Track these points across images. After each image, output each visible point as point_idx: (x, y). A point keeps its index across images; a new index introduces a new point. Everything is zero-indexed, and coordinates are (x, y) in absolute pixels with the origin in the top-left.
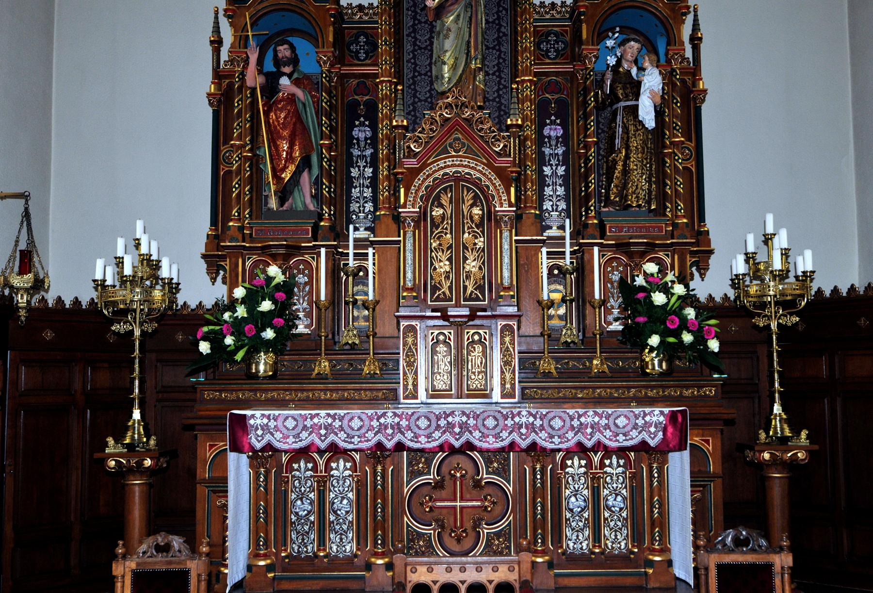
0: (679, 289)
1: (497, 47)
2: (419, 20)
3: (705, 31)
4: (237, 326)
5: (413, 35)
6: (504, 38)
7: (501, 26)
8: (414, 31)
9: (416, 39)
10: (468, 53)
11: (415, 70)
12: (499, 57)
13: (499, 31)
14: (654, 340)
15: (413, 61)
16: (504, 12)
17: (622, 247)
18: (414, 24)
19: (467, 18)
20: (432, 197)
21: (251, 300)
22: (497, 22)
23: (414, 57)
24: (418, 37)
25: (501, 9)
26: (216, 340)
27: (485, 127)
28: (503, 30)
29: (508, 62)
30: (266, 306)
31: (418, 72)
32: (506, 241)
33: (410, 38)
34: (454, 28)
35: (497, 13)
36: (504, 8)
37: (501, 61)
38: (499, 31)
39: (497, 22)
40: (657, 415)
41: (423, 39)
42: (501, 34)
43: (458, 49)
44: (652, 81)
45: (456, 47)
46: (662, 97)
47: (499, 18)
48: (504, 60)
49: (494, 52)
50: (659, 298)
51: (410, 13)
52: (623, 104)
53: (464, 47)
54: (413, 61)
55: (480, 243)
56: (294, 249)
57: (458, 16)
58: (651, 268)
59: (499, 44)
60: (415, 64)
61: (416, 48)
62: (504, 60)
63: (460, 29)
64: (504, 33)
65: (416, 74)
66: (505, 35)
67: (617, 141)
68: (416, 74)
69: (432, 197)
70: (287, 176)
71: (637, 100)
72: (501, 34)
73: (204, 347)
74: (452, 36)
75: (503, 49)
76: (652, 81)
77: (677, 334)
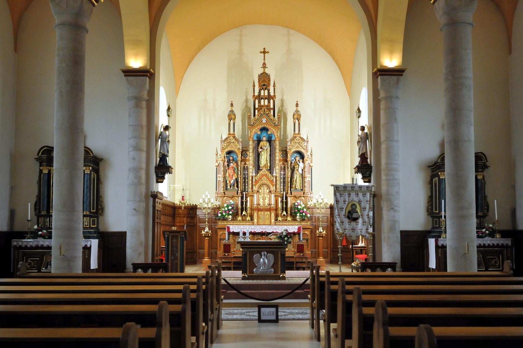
0: (303, 206)
3: (313, 153)
4: (225, 211)
14: (298, 214)
17: (295, 197)
20: (260, 187)
21: (227, 206)
26: (221, 213)
30: (230, 208)
32: (273, 196)
40: (297, 227)
44: (301, 165)
50: (299, 207)
55: (268, 196)
56: (233, 196)
58: (299, 201)
69: (260, 187)
70: (232, 182)
73: (220, 215)
77: (302, 213)
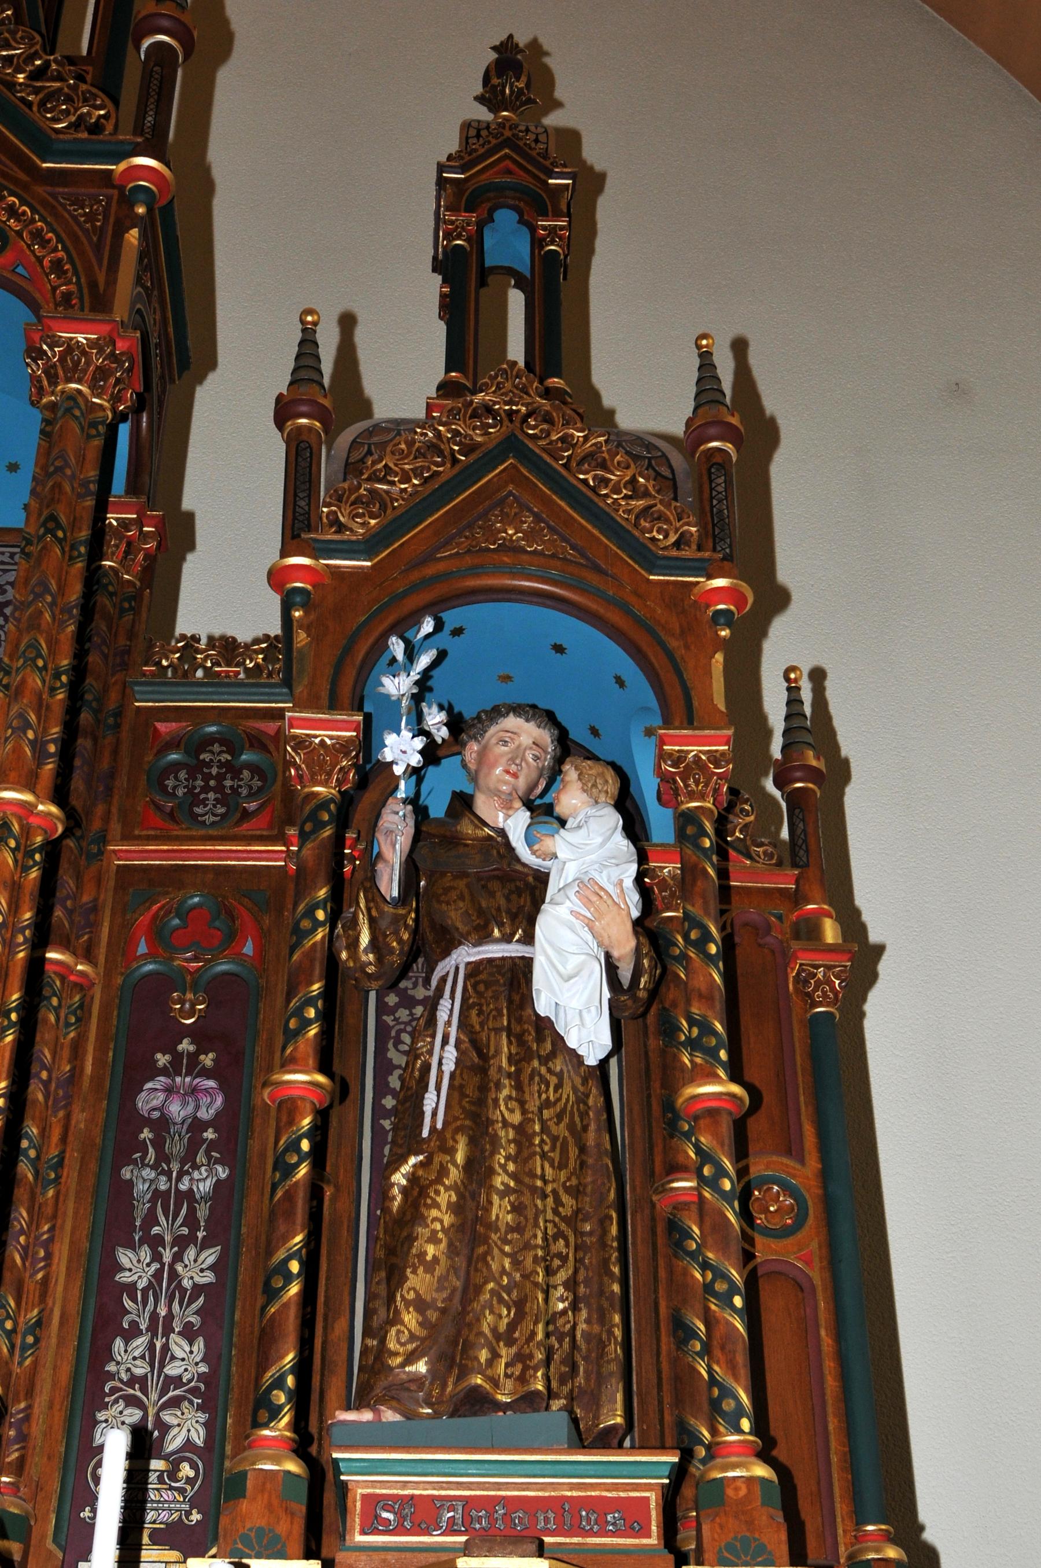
46: (644, 926)
52: (466, 955)
67: (430, 1100)
71: (529, 939)
76: (587, 858)
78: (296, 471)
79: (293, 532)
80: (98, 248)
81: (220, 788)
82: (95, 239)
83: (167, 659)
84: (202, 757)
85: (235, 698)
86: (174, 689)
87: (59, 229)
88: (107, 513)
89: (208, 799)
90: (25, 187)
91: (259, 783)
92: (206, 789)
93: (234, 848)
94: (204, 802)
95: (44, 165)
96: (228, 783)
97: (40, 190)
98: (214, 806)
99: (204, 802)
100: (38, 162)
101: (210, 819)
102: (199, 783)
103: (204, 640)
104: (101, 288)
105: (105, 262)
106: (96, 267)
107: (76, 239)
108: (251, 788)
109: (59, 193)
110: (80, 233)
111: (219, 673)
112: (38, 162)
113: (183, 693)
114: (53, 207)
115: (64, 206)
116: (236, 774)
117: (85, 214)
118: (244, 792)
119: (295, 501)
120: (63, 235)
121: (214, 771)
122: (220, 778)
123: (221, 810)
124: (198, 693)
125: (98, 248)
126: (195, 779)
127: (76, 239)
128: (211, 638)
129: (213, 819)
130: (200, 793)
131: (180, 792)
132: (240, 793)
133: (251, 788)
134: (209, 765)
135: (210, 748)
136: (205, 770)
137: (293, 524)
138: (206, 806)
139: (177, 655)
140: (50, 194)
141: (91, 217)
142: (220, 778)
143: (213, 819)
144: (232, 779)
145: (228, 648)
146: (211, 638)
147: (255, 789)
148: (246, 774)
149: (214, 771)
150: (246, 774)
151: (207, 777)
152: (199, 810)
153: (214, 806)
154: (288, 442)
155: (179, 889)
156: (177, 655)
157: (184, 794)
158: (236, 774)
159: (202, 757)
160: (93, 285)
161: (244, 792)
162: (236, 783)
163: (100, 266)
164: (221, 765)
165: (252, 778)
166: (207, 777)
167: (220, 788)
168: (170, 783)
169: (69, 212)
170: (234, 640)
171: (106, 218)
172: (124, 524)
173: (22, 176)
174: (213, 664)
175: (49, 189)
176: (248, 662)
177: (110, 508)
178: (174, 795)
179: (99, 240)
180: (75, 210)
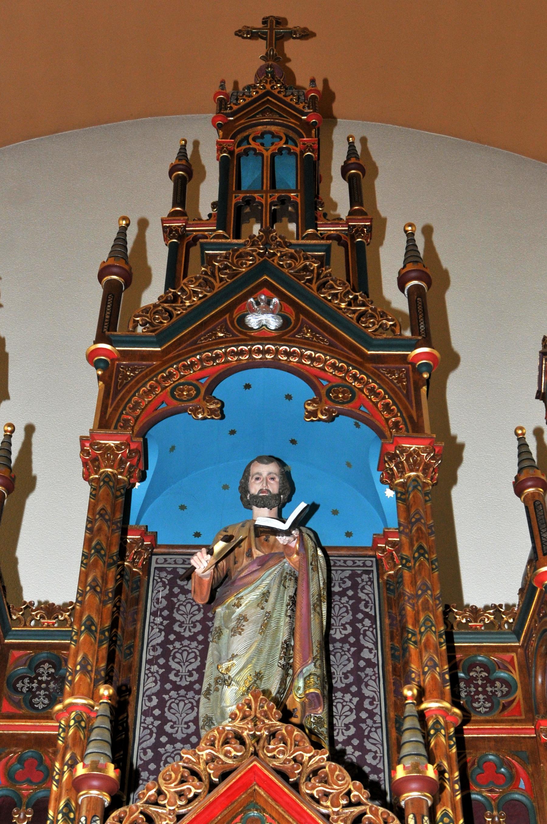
1: (354, 689)
2: (178, 634)
5: (162, 661)
6: (369, 671)
7: (361, 648)
8: (166, 654)
9: (169, 669)
10: (287, 667)
11: (161, 731)
12: (360, 707)
13: (357, 656)
15: (157, 712)
16: (367, 622)
18: (167, 641)
19: (286, 599)
22: (352, 640)
23: (161, 705)
24: (174, 665)
25: (360, 616)
27: (333, 790)
28: (365, 654)
29: (380, 709)
31: (169, 735)
33: (155, 668)
34: (256, 615)
35: (352, 623)
36: (367, 615)
37: (364, 715)
38: (357, 656)
39: (352, 640)
41: (183, 670)
42: (362, 664)
43: (264, 655)
45: (259, 651)
47: (356, 633)
48: (371, 715)
49: (348, 697)
51: (159, 620)
53: (278, 652)
54: (157, 712)
57: (265, 595)
59: (358, 681)
60: (164, 720)
61: (168, 686)
62: (371, 715)
63: (269, 616)
64: (368, 661)
65: (164, 739)
66: (370, 664)
68: (164, 739)
72: (362, 664)
74: (250, 629)
75: (366, 692)
78: (537, 518)
79: (543, 551)
80: (407, 396)
81: (485, 692)
82: (405, 392)
83: (62, 615)
84: (471, 674)
85: (477, 640)
86: (464, 636)
87: (385, 387)
88: (127, 535)
89: (40, 695)
90: (361, 364)
91: (507, 689)
92: (477, 693)
93: (520, 727)
94: (478, 700)
95: (369, 352)
96: (489, 689)
97: (370, 366)
98: (484, 702)
99: (478, 700)
100: (366, 351)
101: (483, 710)
102: (473, 689)
103: (36, 604)
104: (415, 417)
105: (414, 405)
106: (409, 407)
107: (395, 393)
108: (502, 692)
109: (382, 368)
110: (397, 389)
111: (471, 626)
112: (366, 351)
113: (470, 638)
114: (379, 375)
115: (384, 374)
116: (493, 685)
117: (396, 379)
118: (499, 694)
119: (540, 535)
120: (388, 390)
121: (480, 682)
122: (484, 686)
123: (488, 705)
124: (465, 638)
125: (407, 396)
126: (470, 687)
127: (395, 393)
128: (40, 603)
129: (485, 710)
130: (36, 691)
131: (25, 690)
132: (497, 695)
133: (502, 692)
134: (476, 679)
135: (474, 669)
136: (475, 682)
137: (543, 547)
138: (479, 702)
139: (68, 614)
140: (375, 368)
141: (400, 380)
142: (484, 686)
143: (485, 710)
144: (491, 687)
145: (50, 610)
146: (40, 603)
147: (505, 693)
148: (498, 684)
149: (480, 682)
150: (498, 684)
151: (476, 686)
152: (476, 705)
153: (484, 702)
154: (524, 502)
155: (477, 751)
156: (68, 614)
157: (466, 696)
158: (493, 685)
159: (471, 674)
160: (411, 417)
161: (499, 694)
162: (493, 689)
163: (412, 408)
164: (483, 679)
165: (502, 686)
166: (476, 686)
167: (485, 692)
168: (20, 685)
169: (387, 377)
170: (476, 607)
171: (408, 381)
172: (134, 541)
173: (358, 358)
174: (41, 617)
175: (374, 365)
176: (60, 617)
177: (129, 532)
178: (22, 692)
179: (407, 392)
180: (391, 376)
